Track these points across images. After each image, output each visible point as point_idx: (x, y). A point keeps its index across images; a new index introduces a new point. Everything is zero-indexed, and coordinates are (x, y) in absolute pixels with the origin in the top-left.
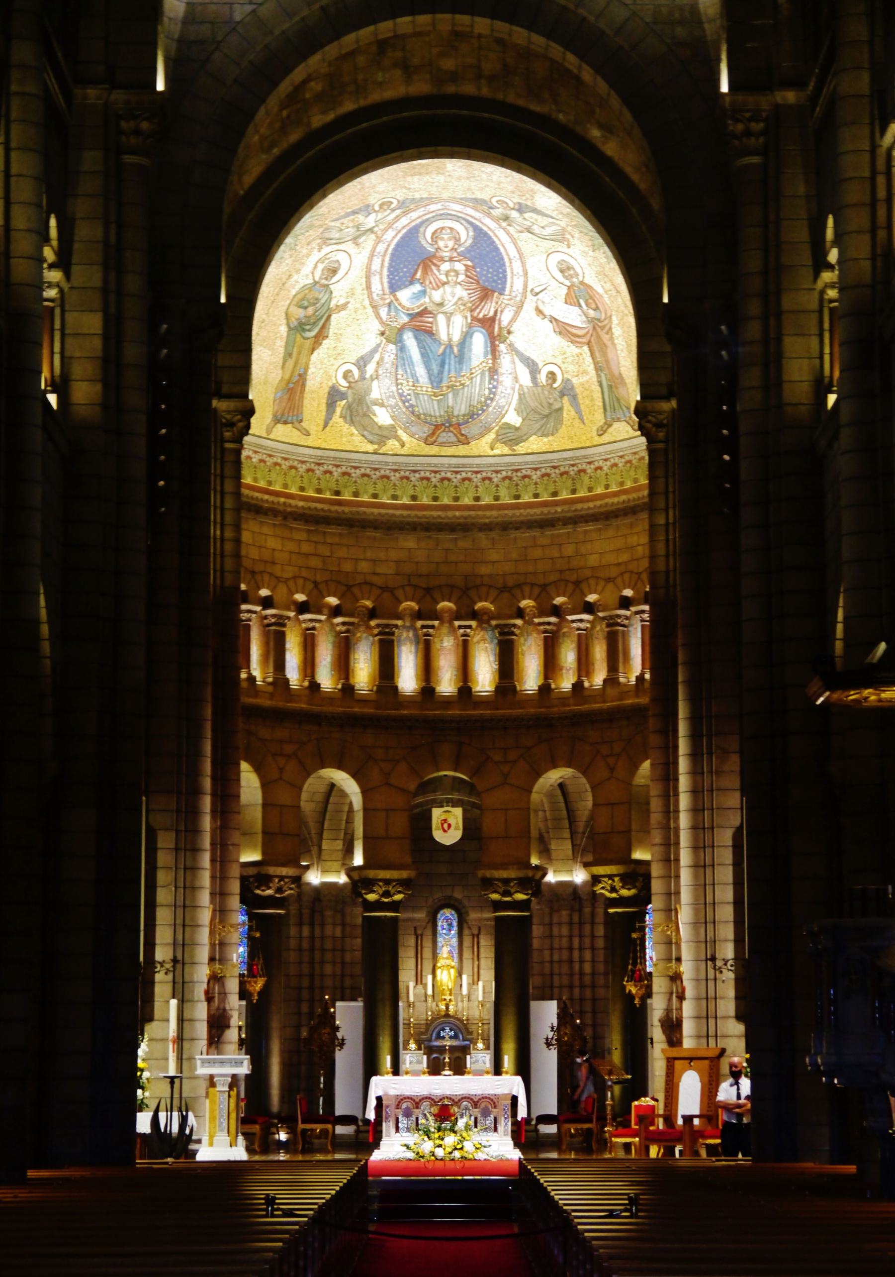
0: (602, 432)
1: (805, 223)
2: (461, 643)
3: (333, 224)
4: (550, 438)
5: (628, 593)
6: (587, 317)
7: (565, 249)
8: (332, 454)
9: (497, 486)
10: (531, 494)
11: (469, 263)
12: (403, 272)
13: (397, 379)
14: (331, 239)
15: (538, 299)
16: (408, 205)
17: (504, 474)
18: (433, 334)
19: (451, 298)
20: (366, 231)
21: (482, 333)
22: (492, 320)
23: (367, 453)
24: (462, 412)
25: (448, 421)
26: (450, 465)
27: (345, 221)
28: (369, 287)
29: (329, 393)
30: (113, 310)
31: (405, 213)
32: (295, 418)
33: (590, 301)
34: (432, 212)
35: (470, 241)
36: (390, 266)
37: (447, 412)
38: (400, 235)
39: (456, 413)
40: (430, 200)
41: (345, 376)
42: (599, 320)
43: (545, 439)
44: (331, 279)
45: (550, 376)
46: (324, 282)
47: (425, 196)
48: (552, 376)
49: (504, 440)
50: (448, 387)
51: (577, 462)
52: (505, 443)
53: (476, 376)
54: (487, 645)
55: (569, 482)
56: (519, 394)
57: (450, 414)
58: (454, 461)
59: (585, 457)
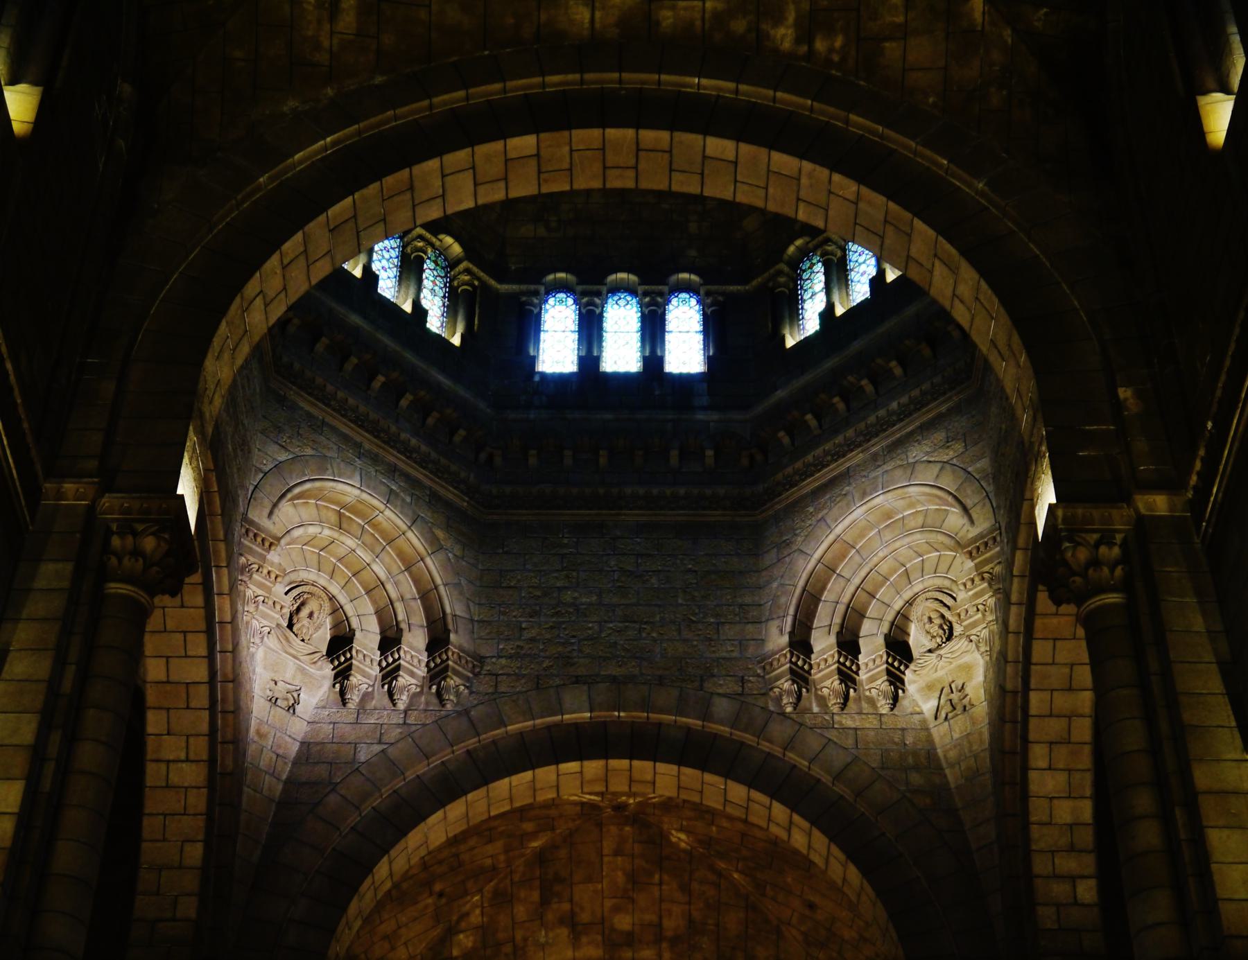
1: (1214, 667)
30: (46, 785)
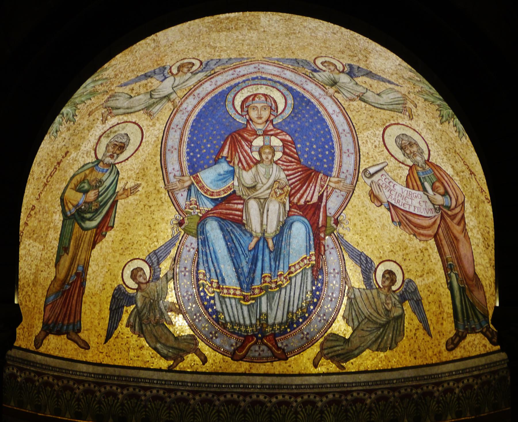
0: (452, 346)
3: (121, 90)
4: (388, 353)
6: (434, 205)
7: (407, 122)
8: (117, 371)
9: (322, 412)
11: (288, 138)
12: (206, 148)
13: (198, 280)
14: (118, 108)
15: (372, 182)
16: (214, 67)
17: (330, 396)
18: (244, 225)
19: (264, 181)
20: (161, 99)
21: (303, 222)
22: (317, 206)
23: (160, 370)
24: (279, 320)
25: (262, 330)
27: (136, 86)
28: (164, 166)
29: (113, 296)
31: (209, 77)
32: (71, 327)
33: (437, 184)
34: (244, 75)
35: (289, 111)
36: (191, 140)
37: (260, 320)
38: (203, 104)
40: (241, 62)
41: (134, 275)
42: (449, 208)
43: (382, 354)
44: (117, 157)
45: (387, 276)
46: (108, 160)
47: (233, 56)
48: (390, 275)
49: (330, 355)
50: (261, 289)
51: (422, 383)
53: (296, 276)
56: (349, 298)
57: (262, 319)
58: (268, 380)
59: (430, 376)
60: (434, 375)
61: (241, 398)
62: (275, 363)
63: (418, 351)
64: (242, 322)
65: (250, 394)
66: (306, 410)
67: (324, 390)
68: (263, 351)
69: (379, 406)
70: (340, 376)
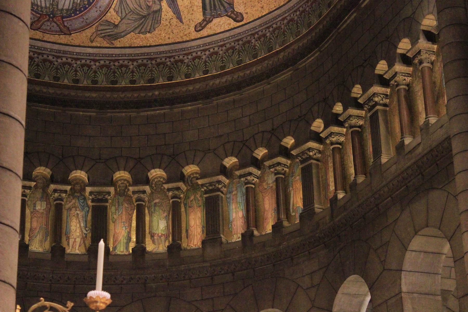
0: (200, 28)
2: (53, 208)
4: (148, 35)
5: (230, 161)
9: (95, 72)
10: (128, 81)
17: (102, 62)
24: (66, 7)
25: (52, 13)
26: (52, 50)
37: (52, 5)
39: (60, 7)
43: (142, 36)
49: (103, 35)
52: (103, 37)
54: (78, 212)
55: (167, 70)
58: (56, 47)
59: (182, 50)
60: (185, 48)
61: (36, 55)
62: (61, 36)
63: (171, 34)
64: (39, 3)
65: (42, 54)
66: (83, 70)
67: (98, 58)
68: (53, 26)
69: (140, 70)
70: (110, 49)
